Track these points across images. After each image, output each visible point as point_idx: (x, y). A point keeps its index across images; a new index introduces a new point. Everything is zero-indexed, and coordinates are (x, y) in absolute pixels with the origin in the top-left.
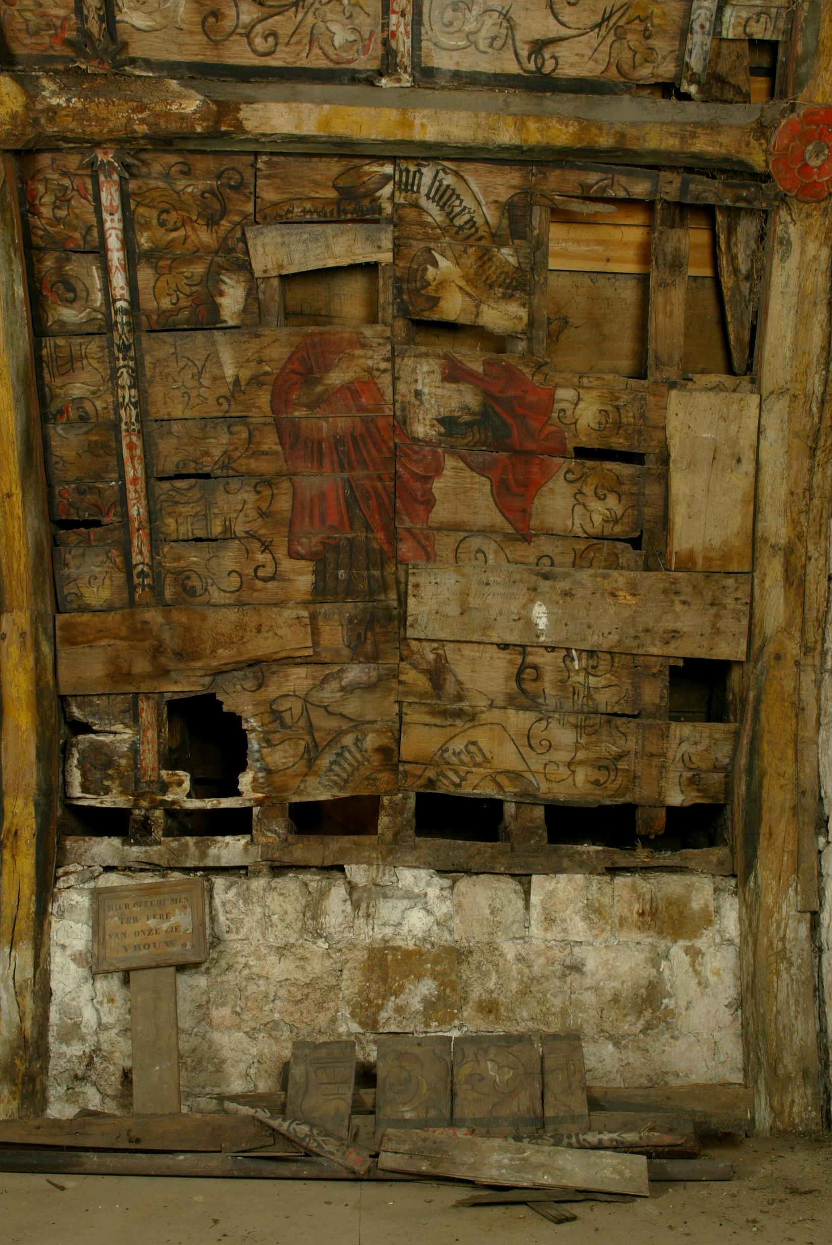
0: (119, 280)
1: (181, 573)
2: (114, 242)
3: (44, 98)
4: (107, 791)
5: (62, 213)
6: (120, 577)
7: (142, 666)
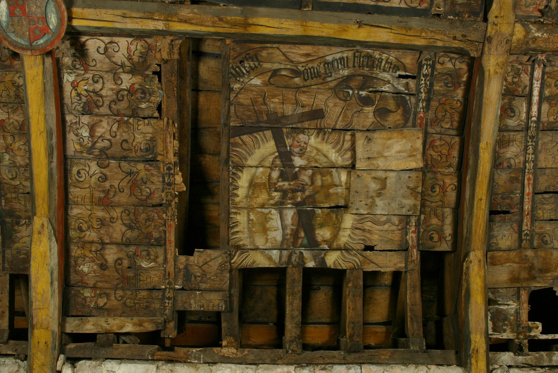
0: (535, 108)
1: (542, 234)
2: (536, 93)
3: (533, 33)
4: (505, 331)
5: (516, 80)
6: (516, 236)
7: (524, 275)
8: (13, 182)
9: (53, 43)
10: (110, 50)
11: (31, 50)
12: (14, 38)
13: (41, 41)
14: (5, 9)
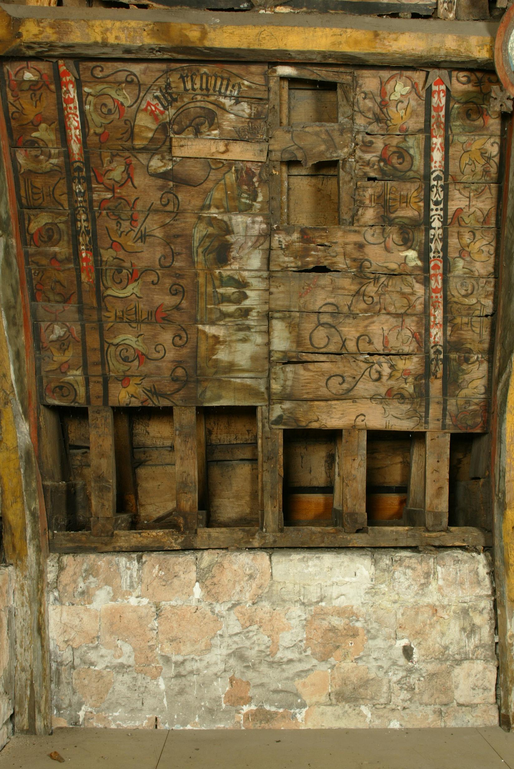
8: (466, 301)
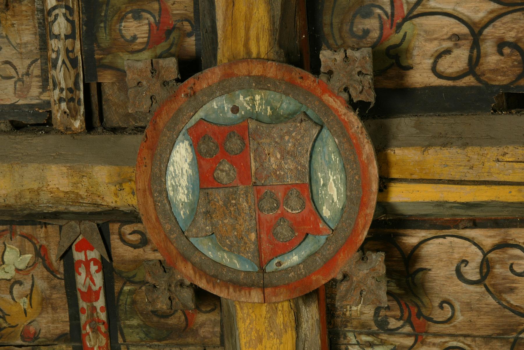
9: (330, 263)
10: (498, 270)
11: (263, 288)
12: (210, 254)
13: (294, 259)
14: (186, 166)
